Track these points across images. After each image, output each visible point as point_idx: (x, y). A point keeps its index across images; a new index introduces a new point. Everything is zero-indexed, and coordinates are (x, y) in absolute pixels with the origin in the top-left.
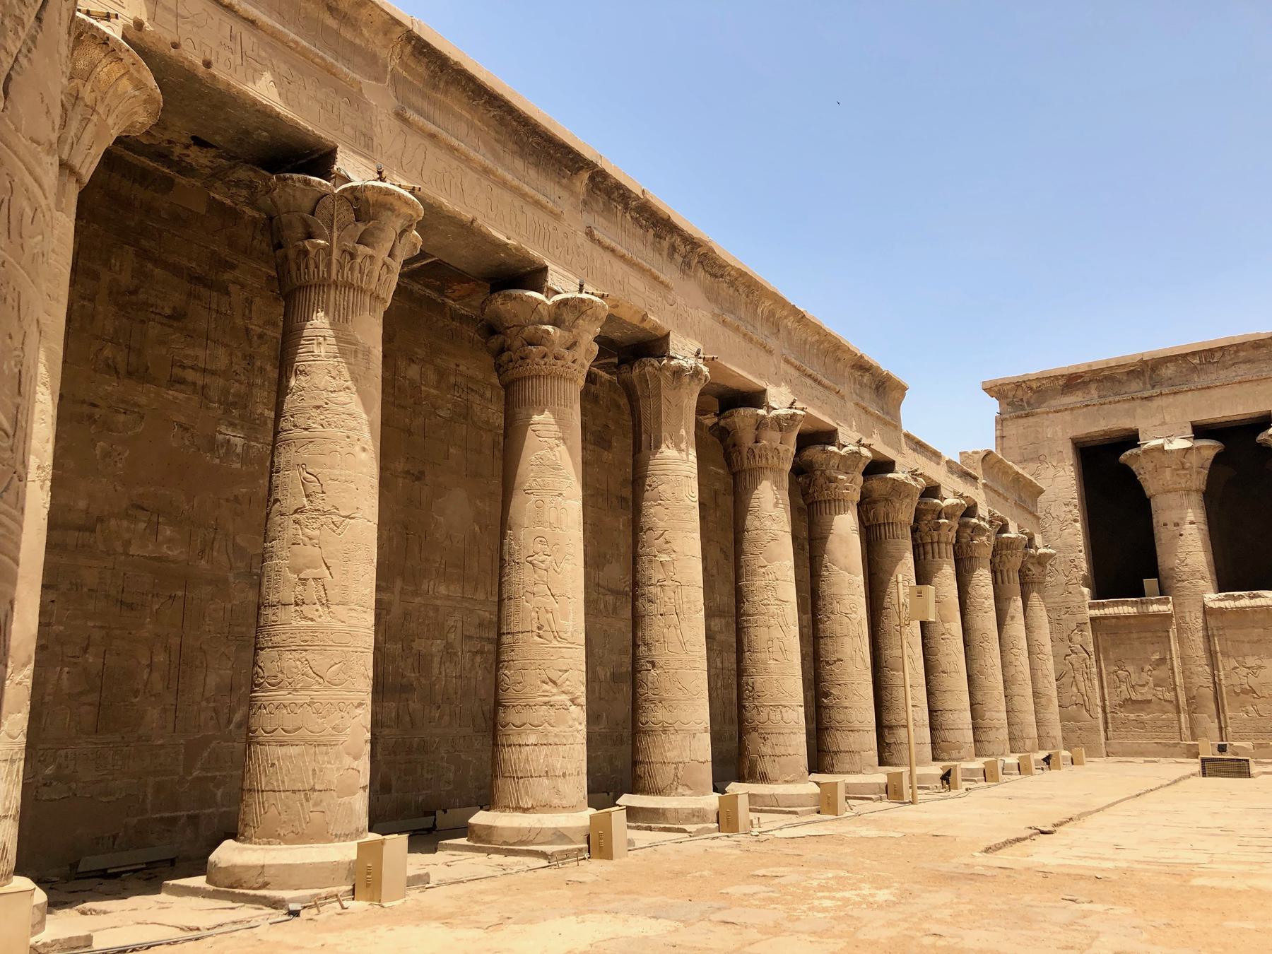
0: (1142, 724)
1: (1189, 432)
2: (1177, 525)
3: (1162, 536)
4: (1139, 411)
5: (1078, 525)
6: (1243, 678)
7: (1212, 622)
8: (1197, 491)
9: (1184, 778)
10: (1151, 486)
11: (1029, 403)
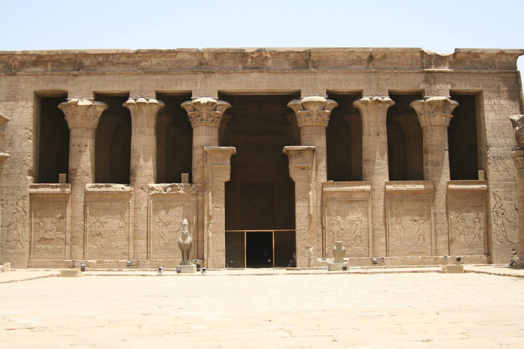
0: (47, 250)
2: (79, 146)
3: (73, 150)
4: (70, 81)
6: (97, 228)
7: (87, 199)
8: (92, 129)
9: (39, 278)
10: (71, 124)
11: (15, 68)
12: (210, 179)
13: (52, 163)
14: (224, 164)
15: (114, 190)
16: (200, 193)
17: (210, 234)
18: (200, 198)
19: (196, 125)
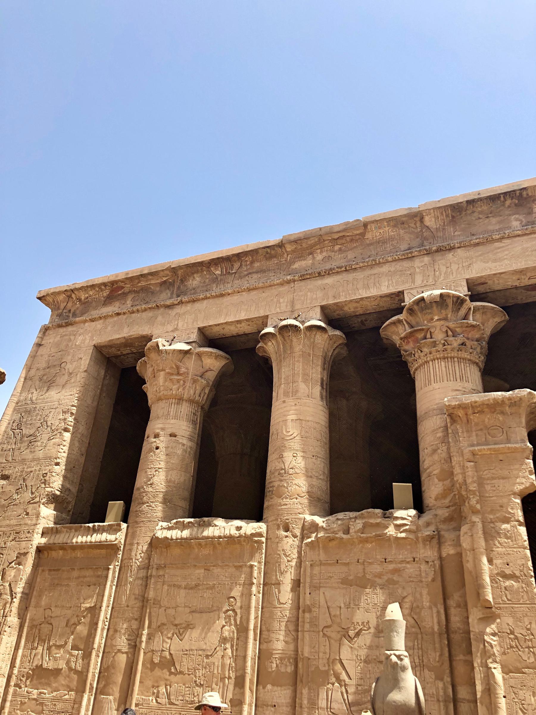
1: (194, 337)
5: (67, 436)
7: (156, 560)
8: (191, 401)
12: (473, 487)
13: (105, 480)
14: (508, 441)
15: (217, 533)
16: (448, 536)
17: (498, 674)
18: (448, 550)
19: (420, 361)
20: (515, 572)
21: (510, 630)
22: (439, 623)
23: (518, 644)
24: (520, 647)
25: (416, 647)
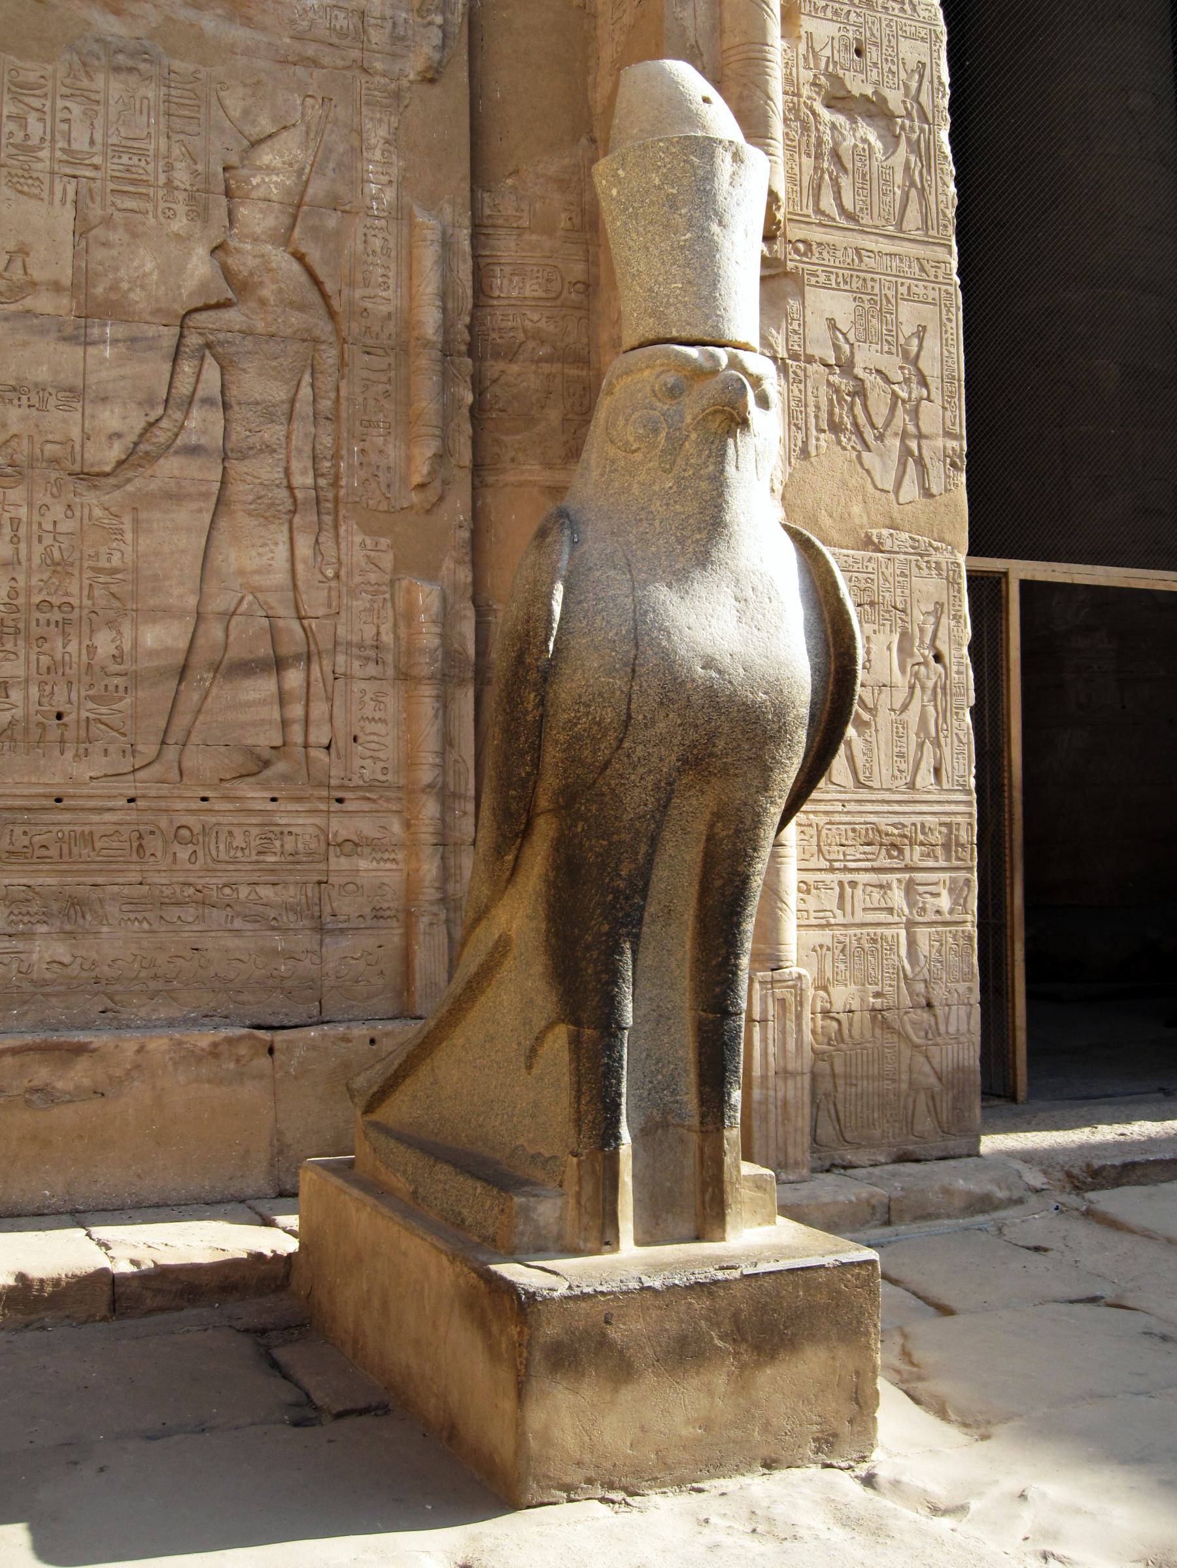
20: (887, 92)
21: (837, 348)
22: (444, 295)
23: (862, 419)
24: (869, 435)
25: (304, 406)
